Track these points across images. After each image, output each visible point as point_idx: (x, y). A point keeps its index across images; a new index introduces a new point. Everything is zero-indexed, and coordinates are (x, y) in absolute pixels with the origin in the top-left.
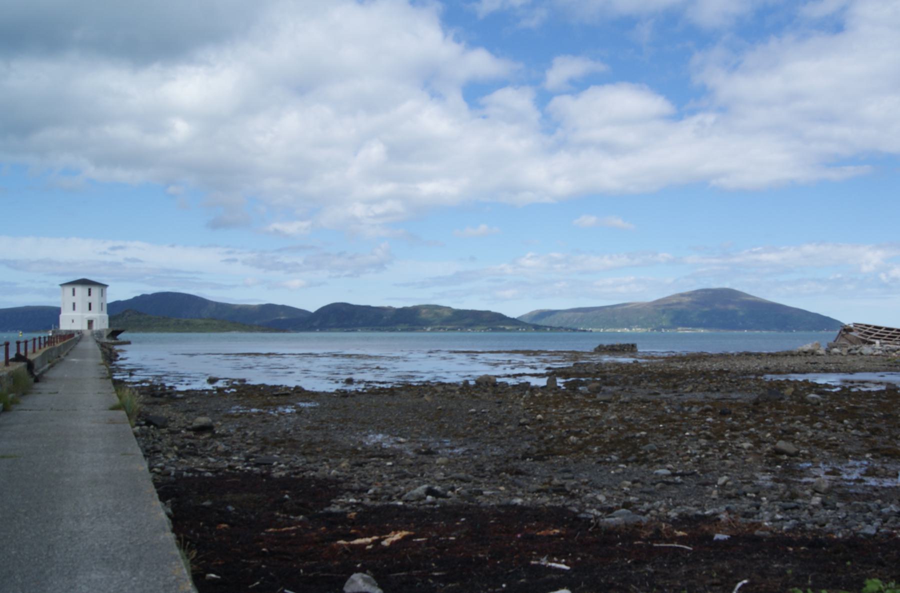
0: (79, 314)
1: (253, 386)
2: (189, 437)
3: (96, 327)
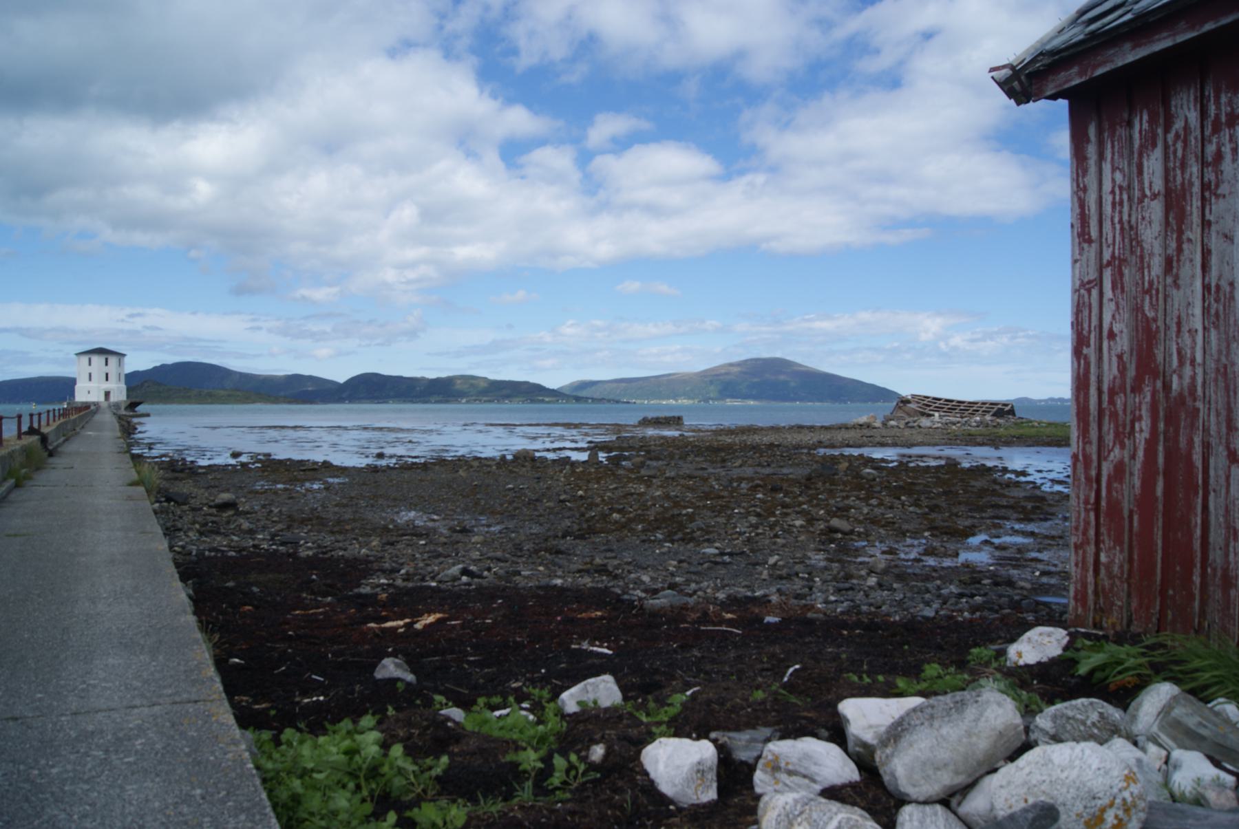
2: (211, 515)
3: (113, 399)
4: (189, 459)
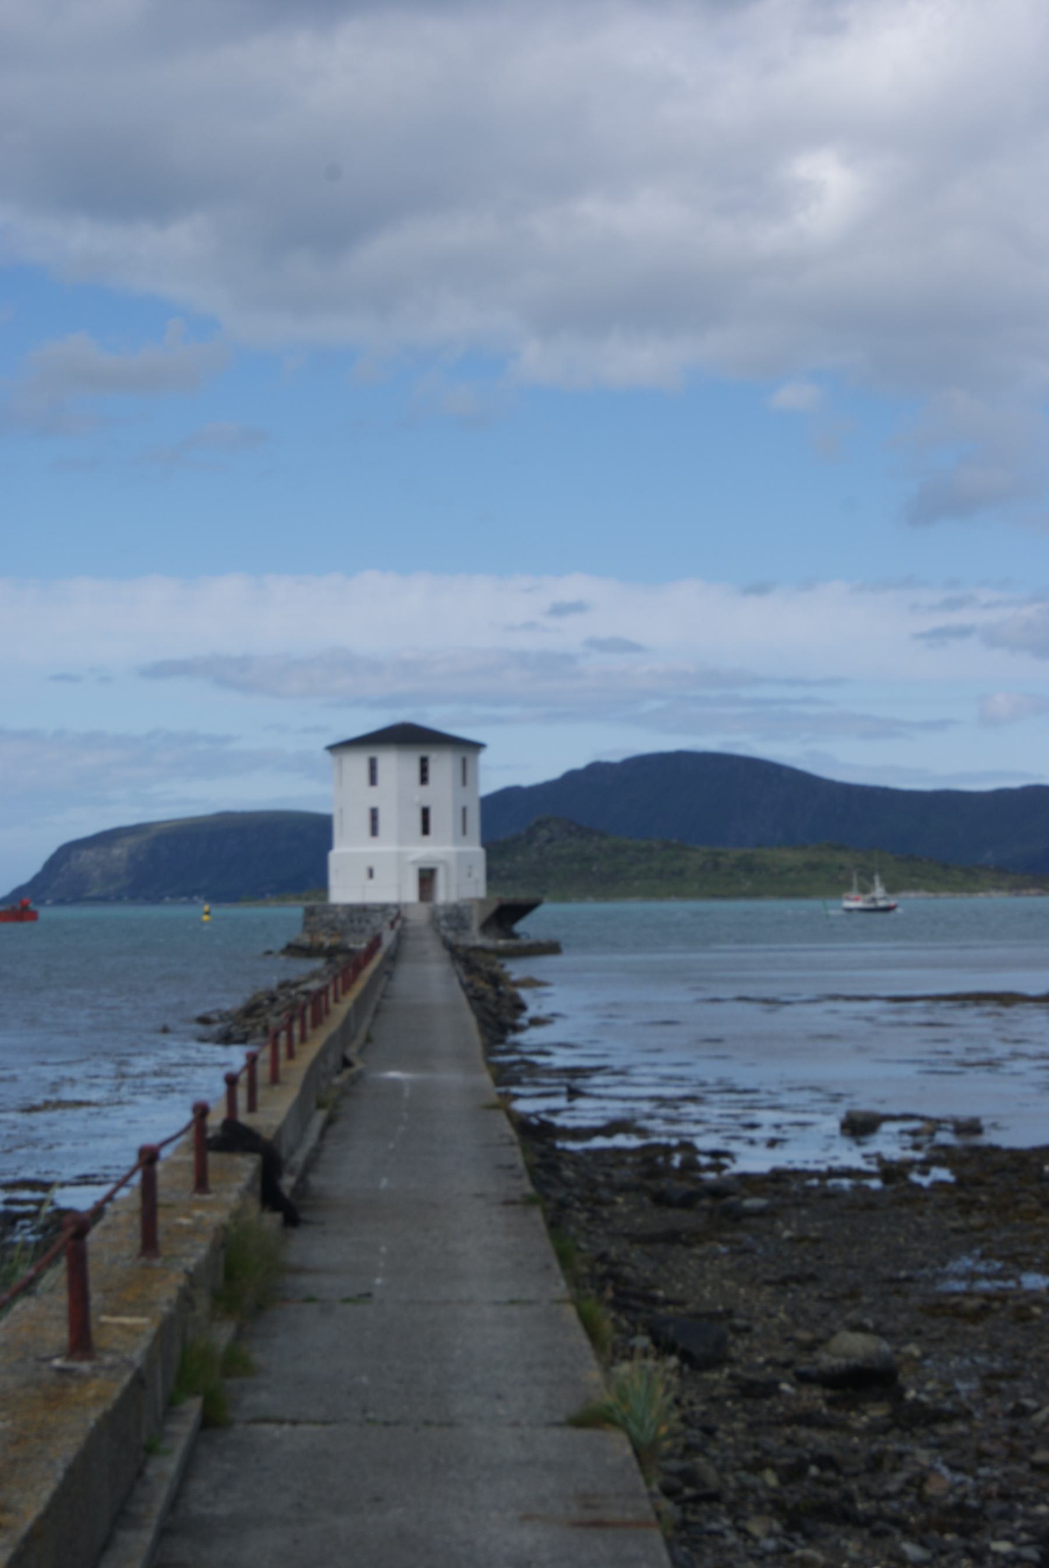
0: (393, 848)
1: (1012, 1152)
2: (807, 1419)
3: (445, 894)
4: (706, 1143)
